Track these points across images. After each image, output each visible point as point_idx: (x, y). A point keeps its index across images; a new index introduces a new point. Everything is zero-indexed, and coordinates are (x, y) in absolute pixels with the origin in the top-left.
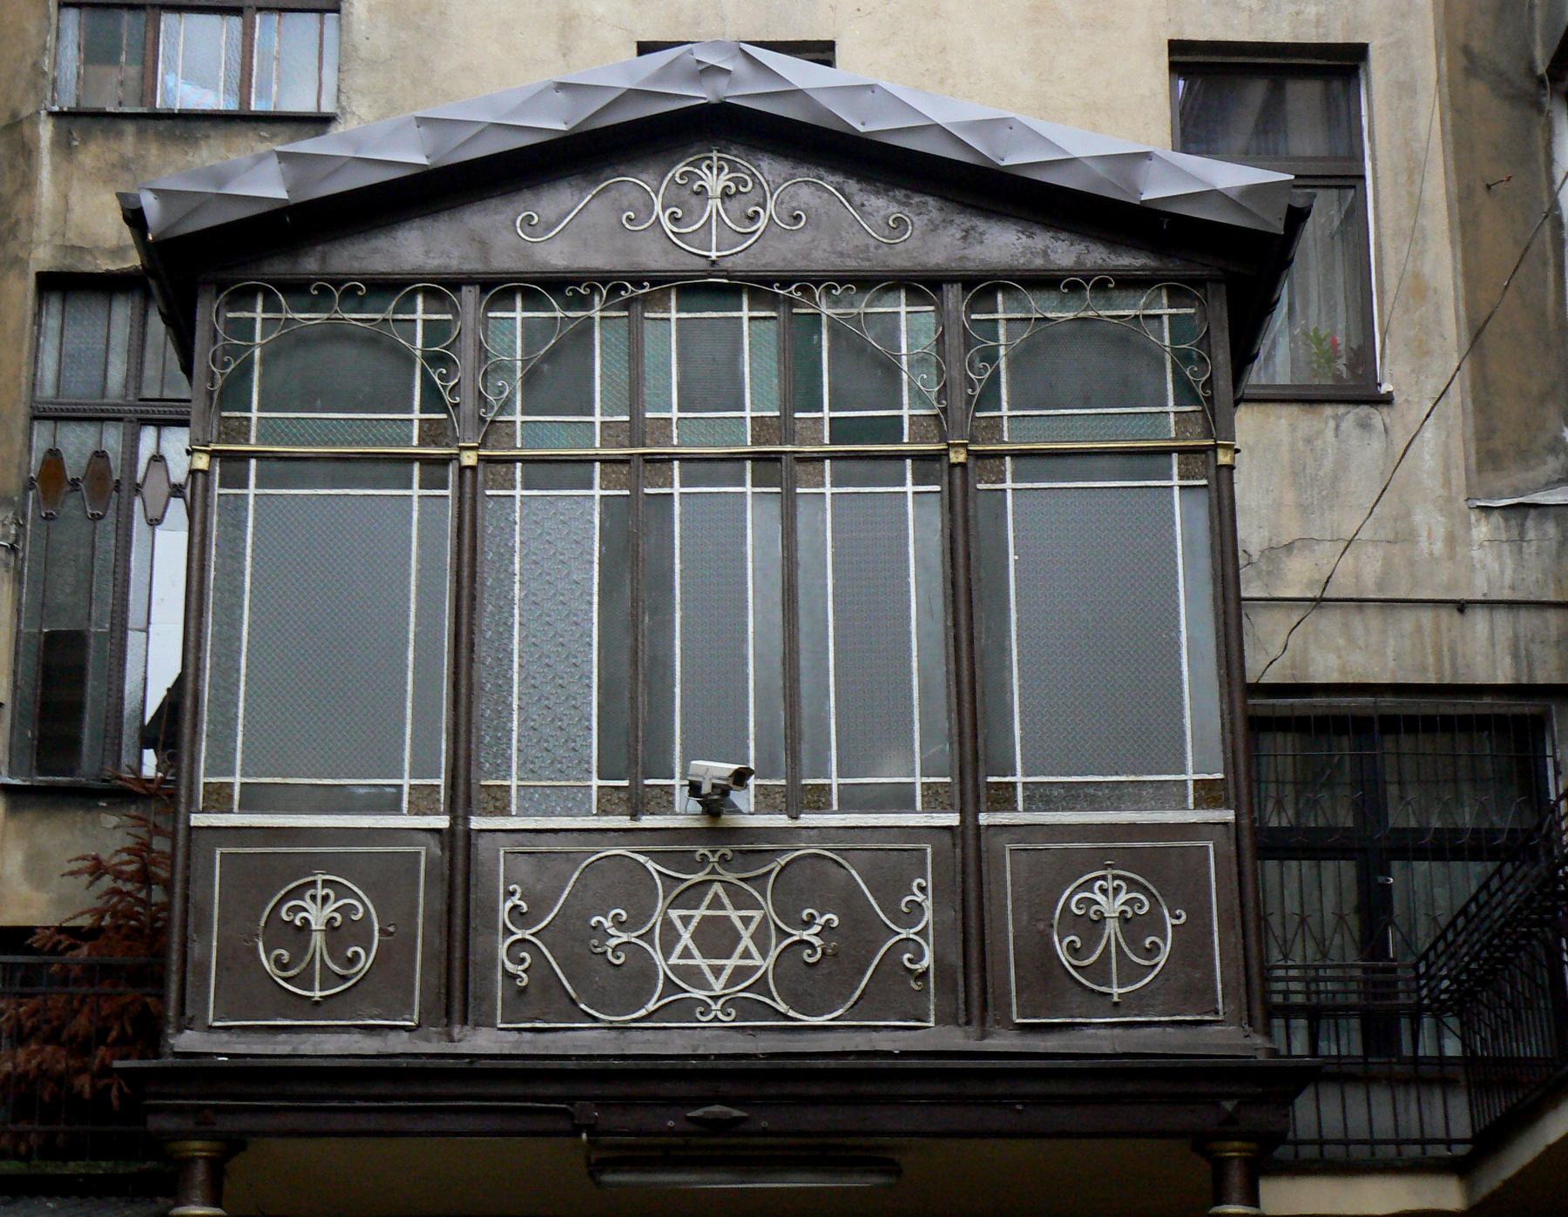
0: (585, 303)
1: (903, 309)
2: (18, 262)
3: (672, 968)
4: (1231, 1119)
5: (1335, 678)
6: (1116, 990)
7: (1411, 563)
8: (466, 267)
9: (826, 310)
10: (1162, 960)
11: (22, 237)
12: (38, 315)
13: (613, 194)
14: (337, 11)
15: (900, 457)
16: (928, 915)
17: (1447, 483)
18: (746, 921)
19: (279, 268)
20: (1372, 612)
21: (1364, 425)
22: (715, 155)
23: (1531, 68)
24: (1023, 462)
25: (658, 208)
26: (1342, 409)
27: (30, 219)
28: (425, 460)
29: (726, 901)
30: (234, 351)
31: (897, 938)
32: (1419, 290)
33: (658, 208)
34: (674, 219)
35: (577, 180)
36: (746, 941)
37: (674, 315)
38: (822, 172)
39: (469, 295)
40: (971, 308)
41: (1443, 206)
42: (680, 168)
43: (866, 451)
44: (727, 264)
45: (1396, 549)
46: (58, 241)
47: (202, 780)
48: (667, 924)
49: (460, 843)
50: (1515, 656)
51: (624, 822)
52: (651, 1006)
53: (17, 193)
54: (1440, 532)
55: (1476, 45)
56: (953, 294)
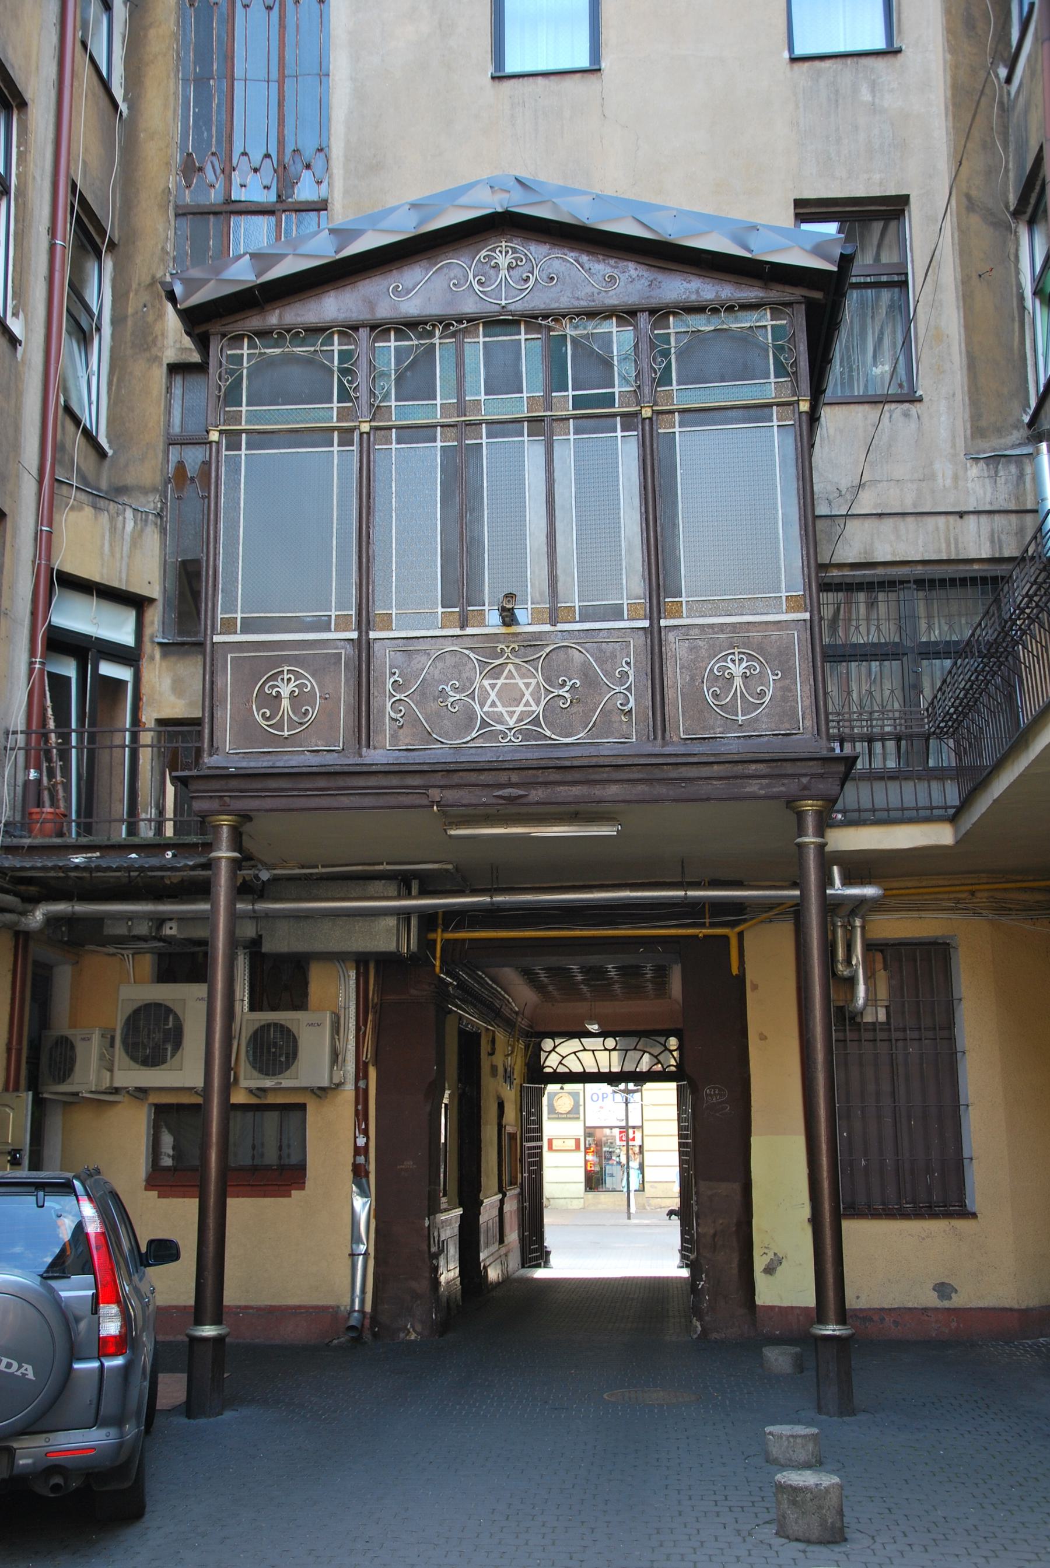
0: (431, 334)
1: (615, 330)
2: (157, 359)
3: (484, 713)
4: (805, 788)
5: (889, 558)
6: (740, 718)
7: (933, 491)
8: (361, 317)
9: (570, 332)
10: (767, 699)
11: (159, 344)
12: (169, 389)
13: (445, 270)
14: (326, 210)
15: (614, 415)
16: (631, 678)
17: (954, 446)
18: (527, 685)
19: (255, 322)
20: (910, 519)
21: (906, 415)
22: (504, 244)
23: (1007, 207)
24: (687, 415)
25: (471, 277)
26: (893, 406)
27: (163, 334)
28: (340, 430)
29: (515, 674)
30: (231, 372)
32: (939, 336)
33: (471, 277)
34: (480, 283)
35: (424, 263)
36: (528, 696)
37: (481, 339)
38: (566, 251)
39: (364, 333)
40: (655, 326)
41: (953, 286)
42: (483, 253)
43: (594, 412)
44: (512, 307)
45: (924, 484)
46: (178, 346)
47: (220, 616)
48: (482, 687)
49: (364, 646)
50: (992, 542)
51: (457, 632)
52: (474, 735)
53: (156, 320)
54: (949, 473)
55: (974, 193)
56: (643, 318)
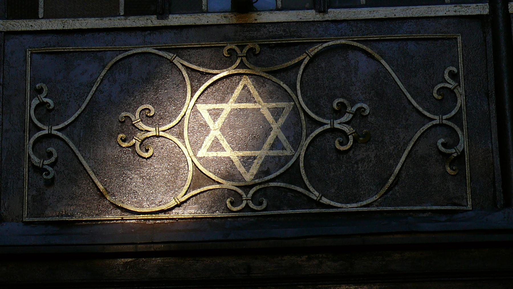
3: (199, 159)
16: (461, 101)
31: (430, 124)
51: (153, 21)
